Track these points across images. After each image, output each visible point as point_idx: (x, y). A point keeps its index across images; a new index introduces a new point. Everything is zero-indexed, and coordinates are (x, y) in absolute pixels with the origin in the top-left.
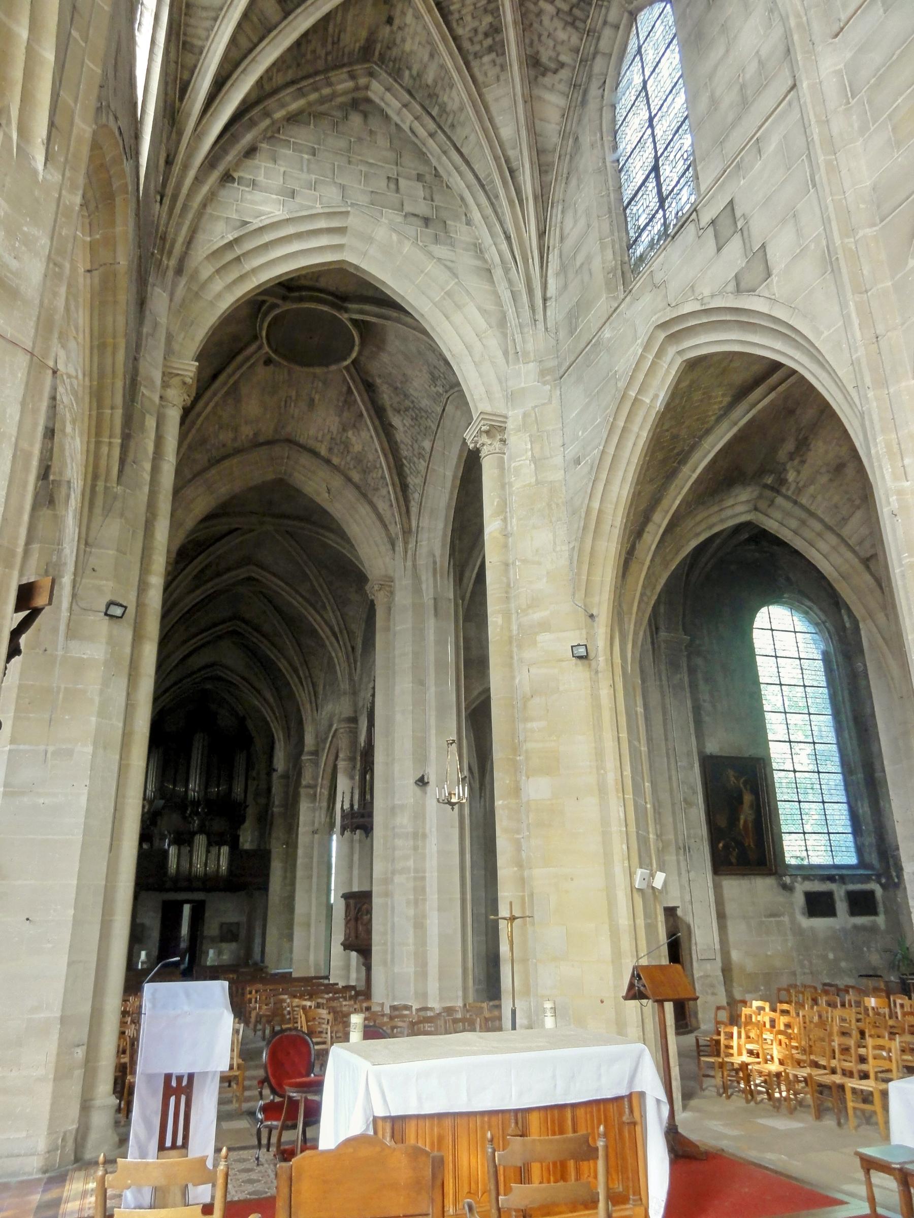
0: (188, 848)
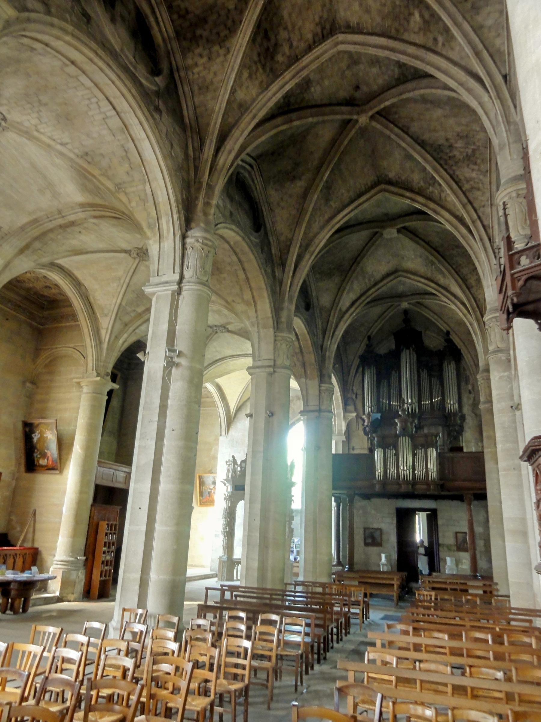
0: (394, 451)
